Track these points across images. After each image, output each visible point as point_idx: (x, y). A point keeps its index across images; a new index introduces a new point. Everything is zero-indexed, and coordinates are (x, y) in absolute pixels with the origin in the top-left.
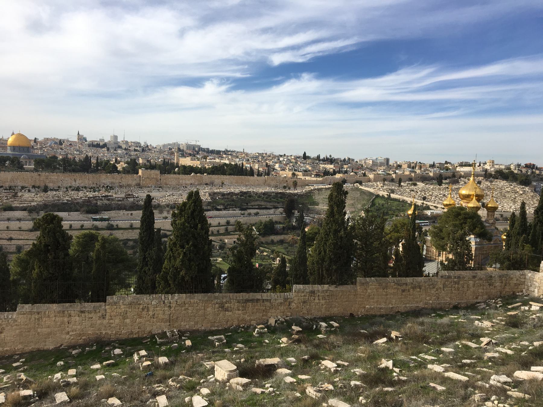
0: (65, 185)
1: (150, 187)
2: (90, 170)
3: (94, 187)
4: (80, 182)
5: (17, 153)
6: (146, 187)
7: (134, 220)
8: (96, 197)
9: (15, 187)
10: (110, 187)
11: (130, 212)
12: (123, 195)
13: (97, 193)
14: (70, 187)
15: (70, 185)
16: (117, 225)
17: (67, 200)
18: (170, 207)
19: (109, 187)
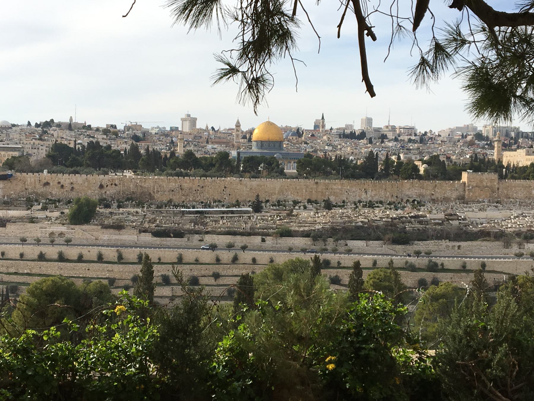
0: (352, 199)
1: (480, 202)
2: (376, 176)
3: (394, 203)
4: (373, 193)
5: (265, 151)
6: (474, 202)
7: (466, 257)
8: (402, 217)
9: (285, 201)
10: (418, 203)
11: (457, 244)
12: (442, 216)
13: (399, 211)
14: (360, 202)
15: (358, 199)
16: (442, 265)
17: (362, 222)
18: (522, 236)
19: (416, 202)
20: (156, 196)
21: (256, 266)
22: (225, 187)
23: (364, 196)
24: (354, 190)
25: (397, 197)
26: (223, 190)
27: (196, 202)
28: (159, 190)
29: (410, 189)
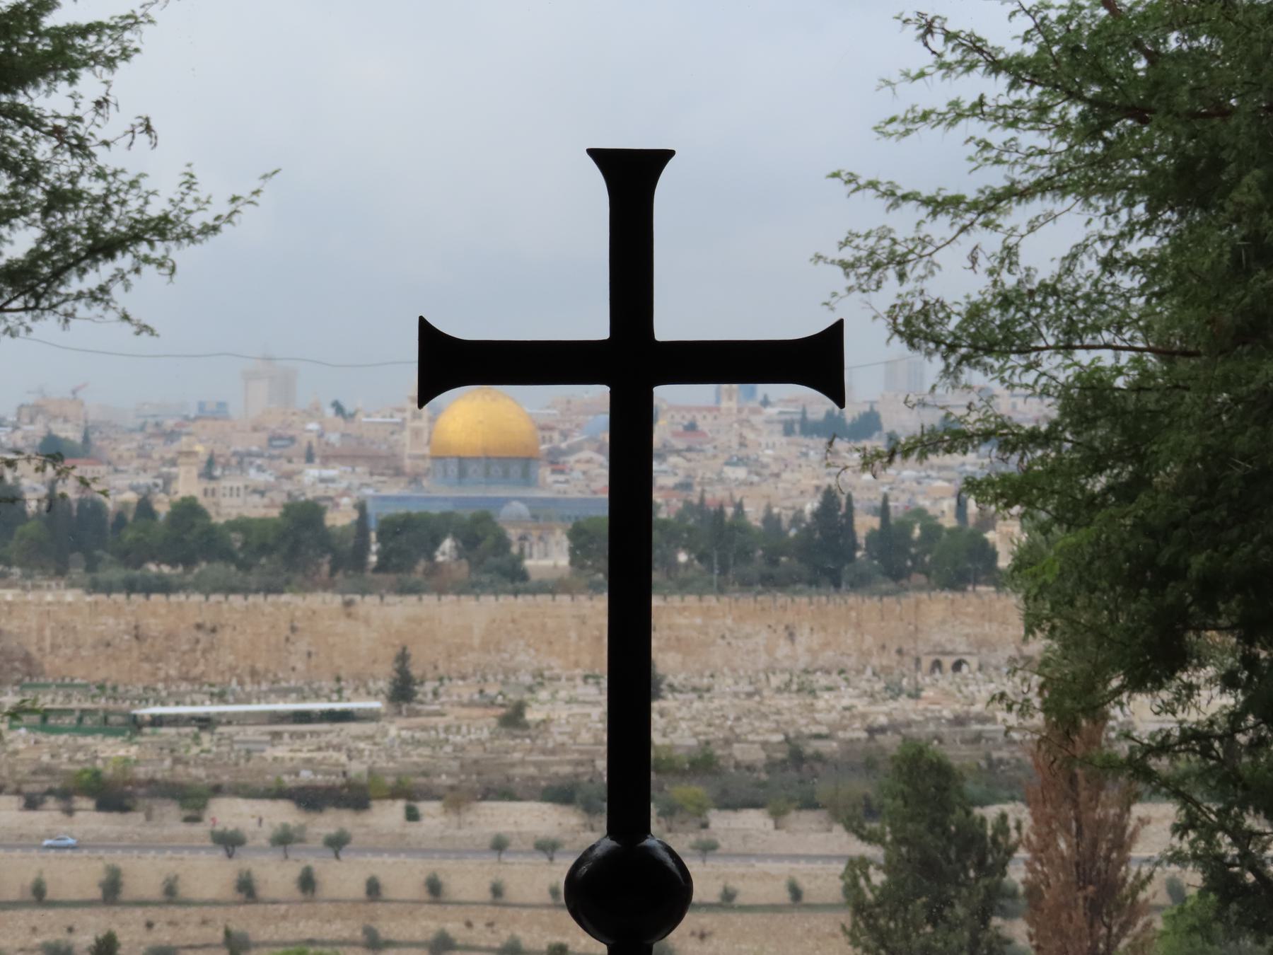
4: (817, 640)
21: (379, 908)
22: (293, 629)
23: (783, 649)
25: (900, 652)
26: (287, 639)
27: (193, 680)
28: (60, 640)
29: (944, 622)
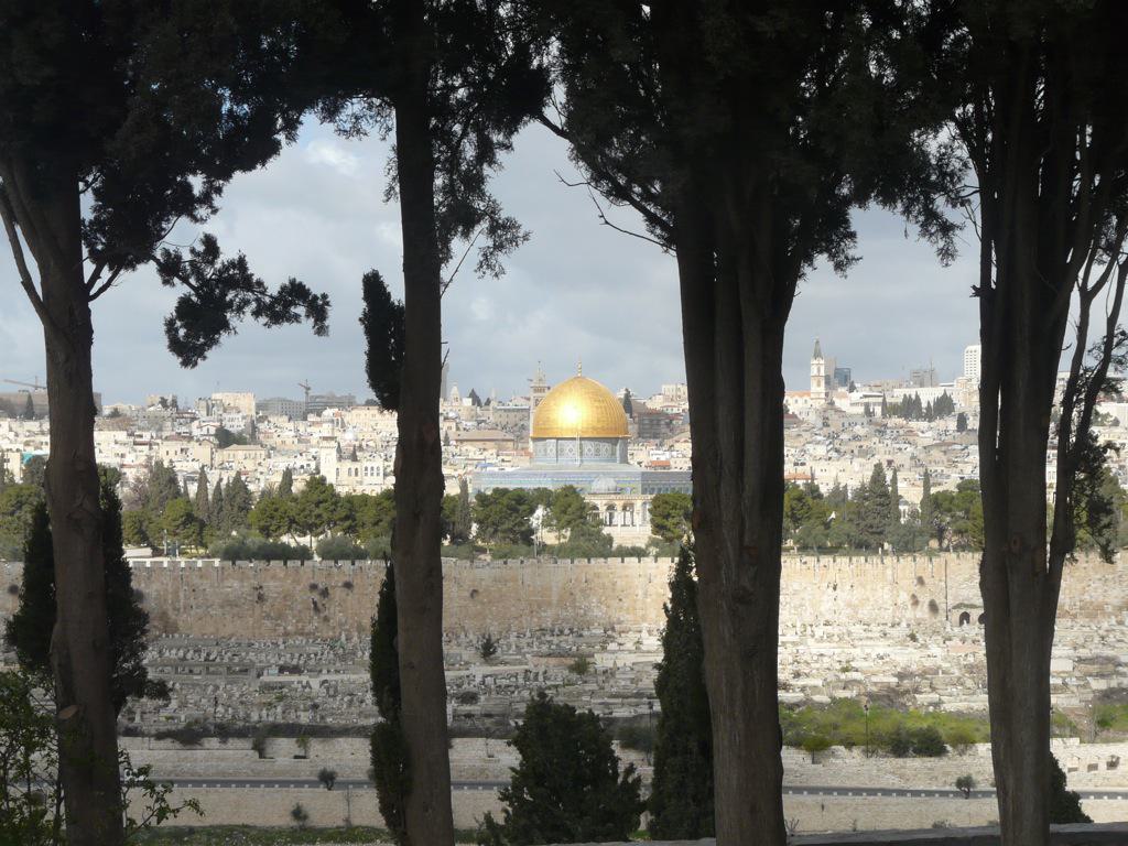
4: (858, 593)
20: (183, 620)
24: (796, 586)
28: (192, 602)
